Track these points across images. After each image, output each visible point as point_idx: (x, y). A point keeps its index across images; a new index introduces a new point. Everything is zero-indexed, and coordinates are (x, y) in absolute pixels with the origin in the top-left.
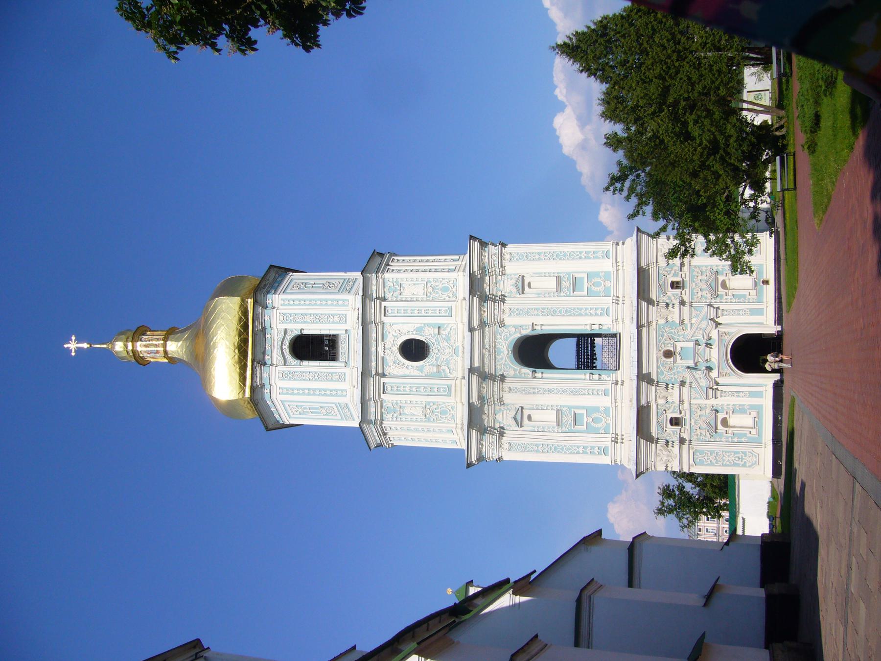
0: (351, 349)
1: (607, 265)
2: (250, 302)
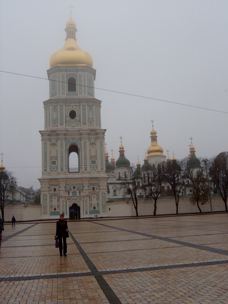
0: (72, 96)
1: (99, 169)
2: (84, 65)
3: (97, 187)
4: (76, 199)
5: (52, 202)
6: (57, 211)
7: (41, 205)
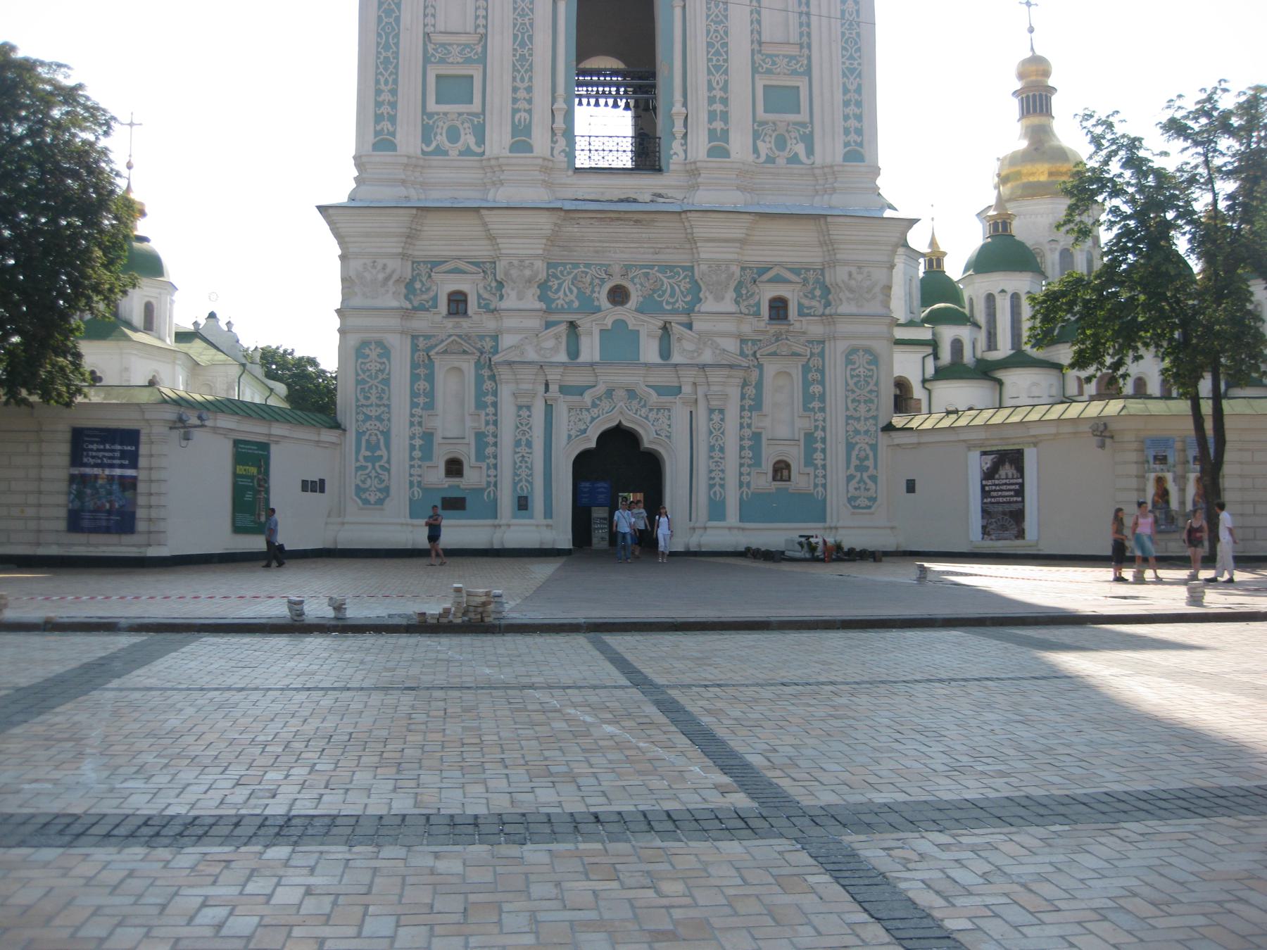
3: (806, 302)
4: (631, 394)
5: (430, 406)
6: (472, 477)
7: (336, 426)
